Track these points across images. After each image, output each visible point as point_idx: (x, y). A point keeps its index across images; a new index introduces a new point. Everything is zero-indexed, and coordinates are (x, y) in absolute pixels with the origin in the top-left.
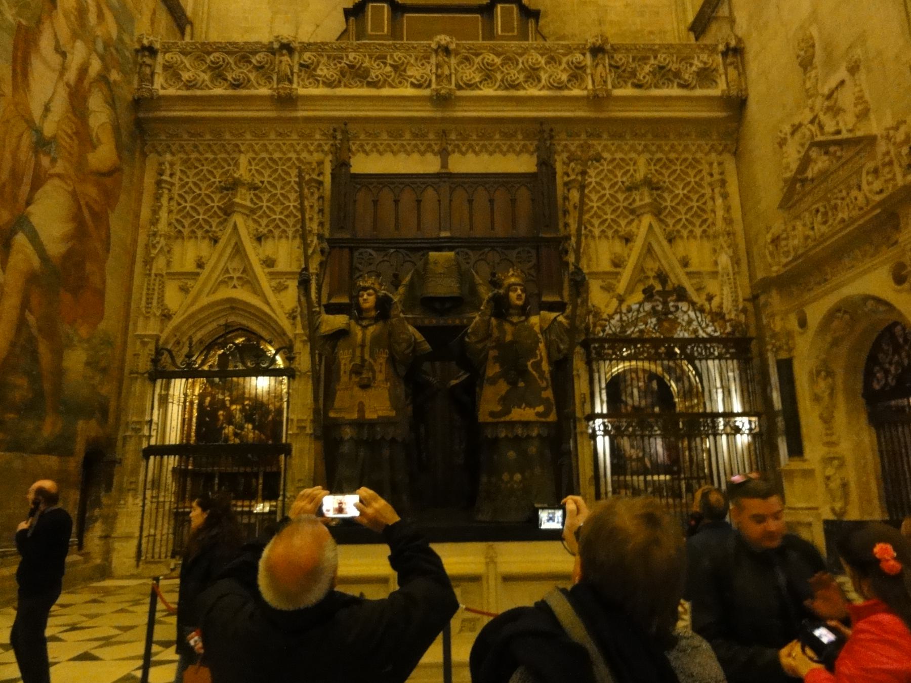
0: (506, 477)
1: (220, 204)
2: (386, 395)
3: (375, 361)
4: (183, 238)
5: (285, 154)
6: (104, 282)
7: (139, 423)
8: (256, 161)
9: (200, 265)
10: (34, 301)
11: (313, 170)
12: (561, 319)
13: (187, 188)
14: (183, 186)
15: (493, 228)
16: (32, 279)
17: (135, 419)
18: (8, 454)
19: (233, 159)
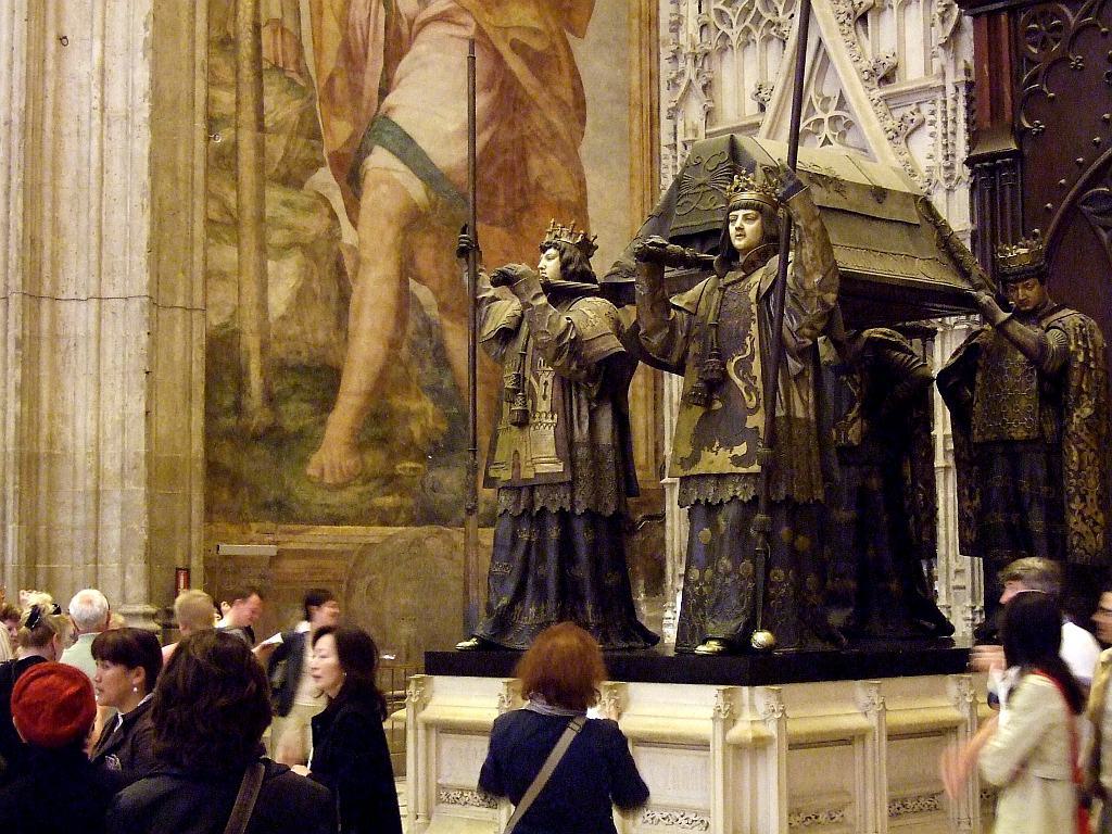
6: (582, 184)
9: (762, 108)
10: (425, 259)
16: (413, 221)
18: (413, 530)
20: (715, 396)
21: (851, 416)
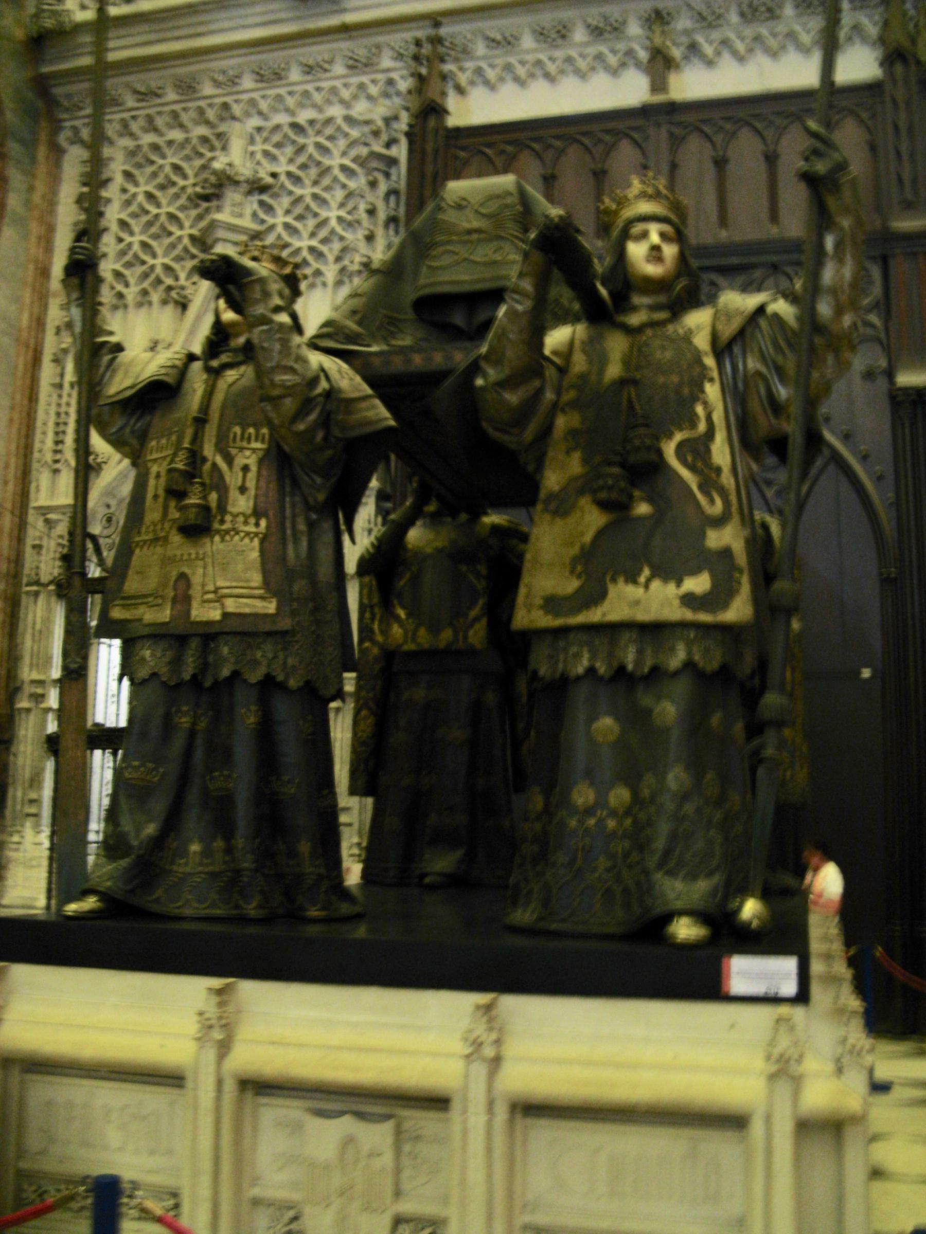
0: (583, 795)
1: (194, 232)
2: (255, 555)
3: (230, 460)
4: (126, 307)
5: (320, 110)
7: (41, 683)
8: (265, 134)
11: (376, 133)
12: (781, 307)
13: (133, 208)
14: (128, 203)
15: (774, 217)
17: (35, 676)
19: (219, 136)
20: (637, 493)
21: (474, 613)
